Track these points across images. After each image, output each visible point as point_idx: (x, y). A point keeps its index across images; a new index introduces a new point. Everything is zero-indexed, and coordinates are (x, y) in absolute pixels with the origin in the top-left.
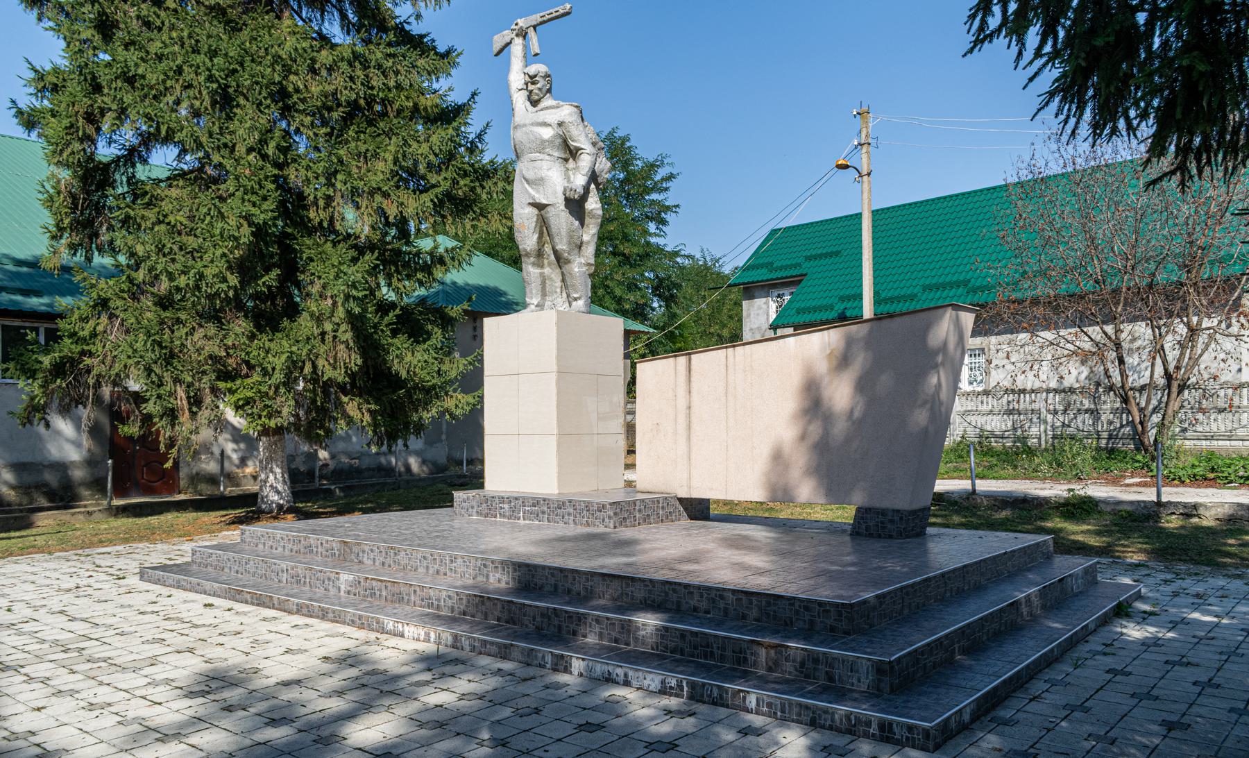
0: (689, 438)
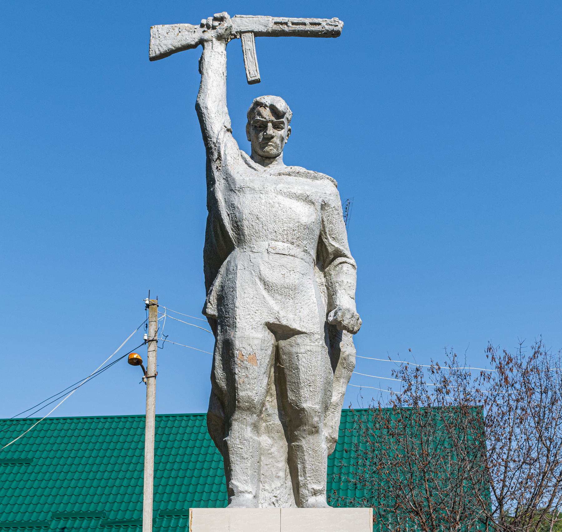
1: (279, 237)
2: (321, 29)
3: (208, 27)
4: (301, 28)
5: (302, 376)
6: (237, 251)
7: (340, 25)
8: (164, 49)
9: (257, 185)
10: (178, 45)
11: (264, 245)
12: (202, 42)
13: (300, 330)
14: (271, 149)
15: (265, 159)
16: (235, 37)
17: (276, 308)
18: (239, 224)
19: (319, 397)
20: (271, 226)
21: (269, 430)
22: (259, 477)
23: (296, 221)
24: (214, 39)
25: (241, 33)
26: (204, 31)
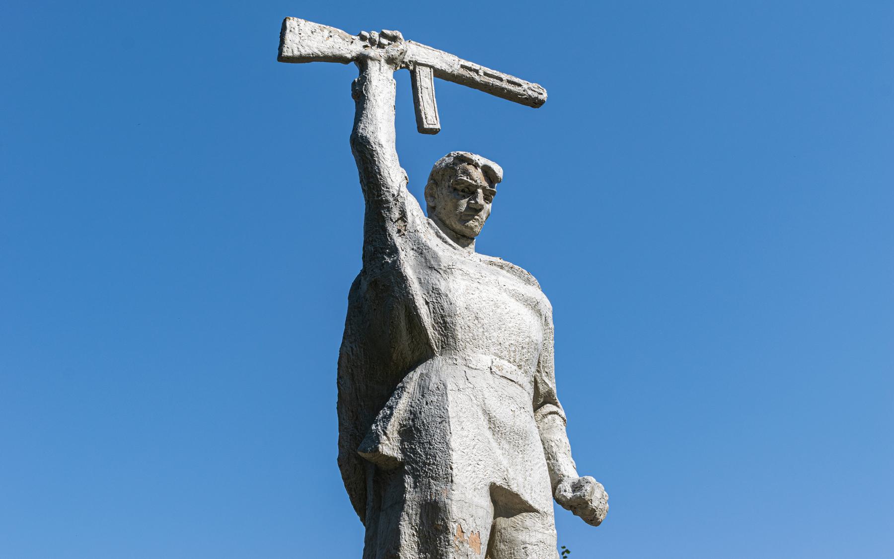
1: (505, 353)
2: (522, 92)
3: (372, 42)
4: (497, 83)
6: (438, 361)
7: (544, 96)
10: (328, 52)
11: (483, 360)
12: (362, 61)
13: (533, 505)
16: (407, 67)
17: (505, 463)
18: (448, 320)
20: (495, 334)
23: (526, 334)
24: (383, 61)
25: (416, 64)
26: (365, 46)
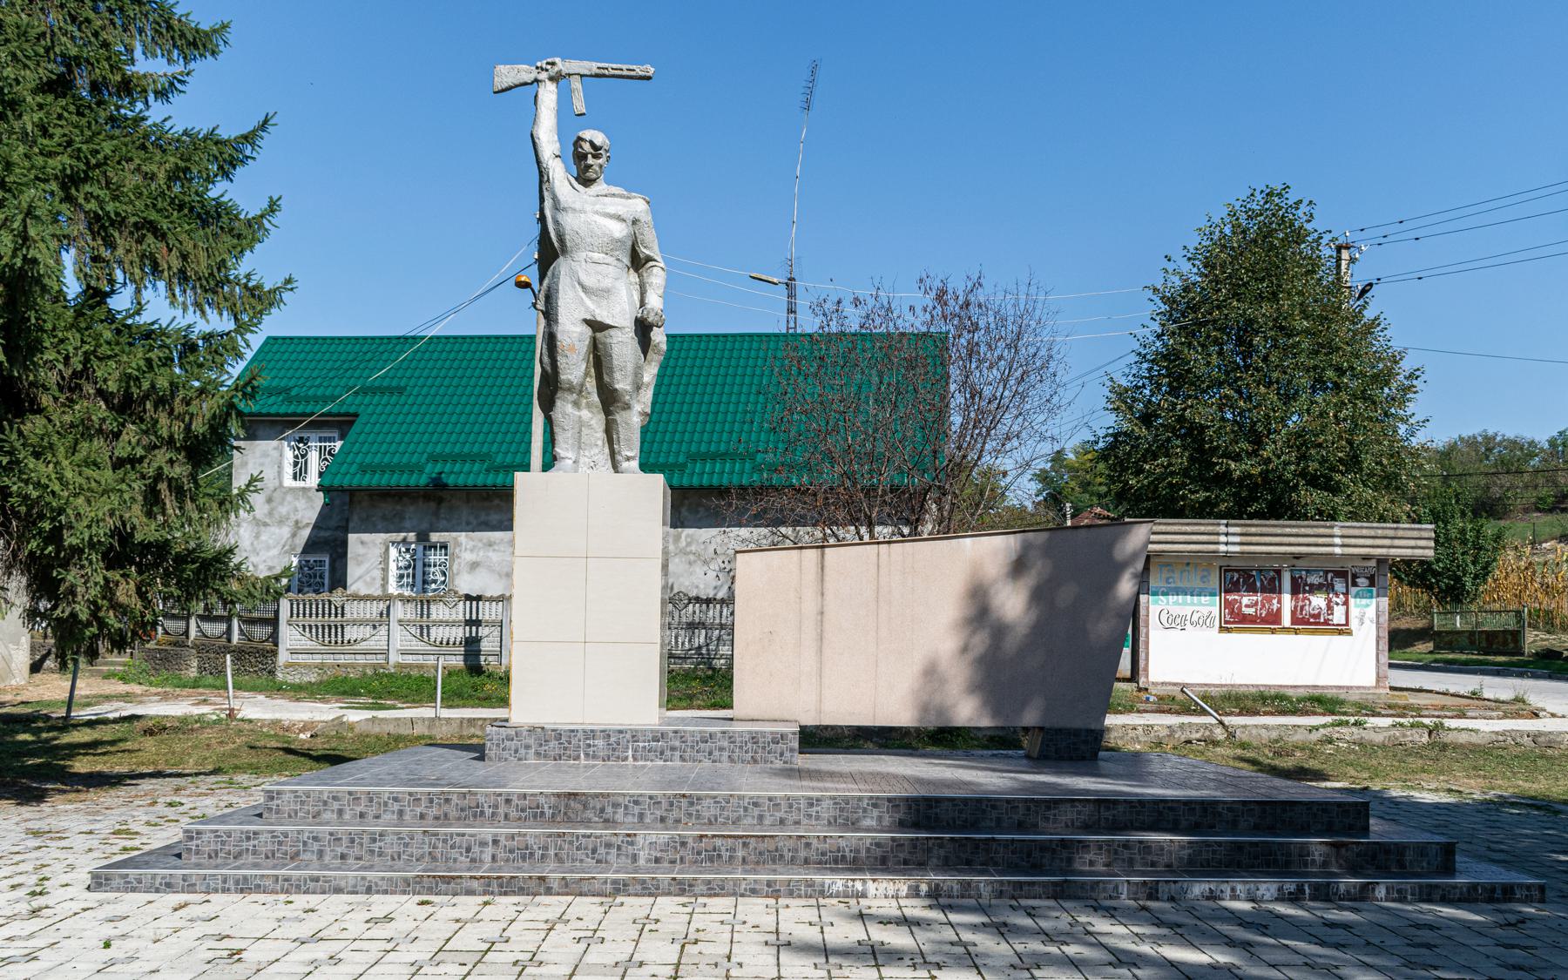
0: (820, 651)
5: (615, 362)
8: (505, 85)
9: (577, 206)
11: (582, 255)
12: (537, 81)
14: (591, 174)
15: (586, 182)
19: (629, 380)
21: (589, 406)
22: (579, 445)
